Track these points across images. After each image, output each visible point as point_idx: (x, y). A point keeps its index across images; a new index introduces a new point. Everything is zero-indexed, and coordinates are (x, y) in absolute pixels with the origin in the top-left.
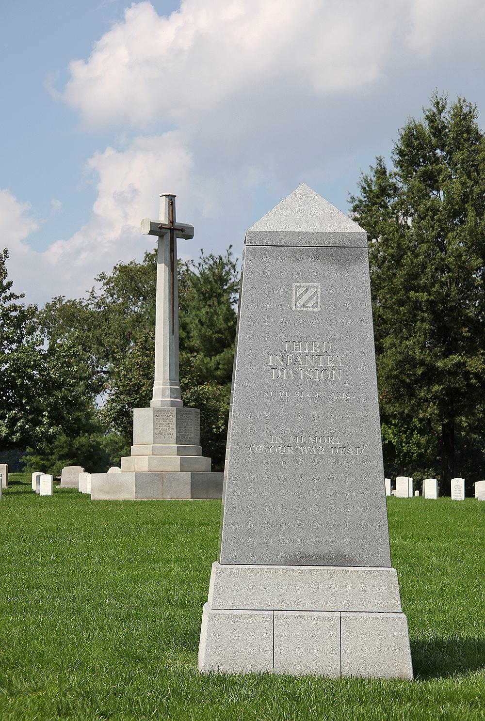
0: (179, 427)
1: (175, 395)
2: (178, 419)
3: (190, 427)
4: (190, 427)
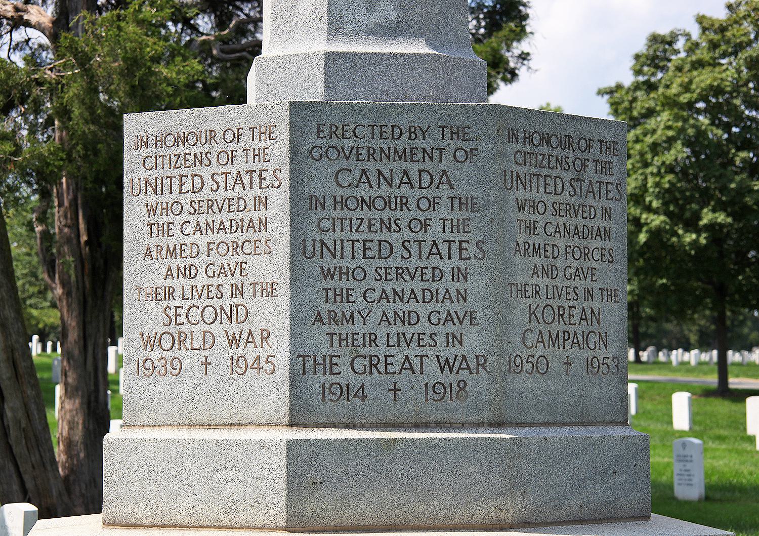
0: (328, 274)
1: (388, 12)
2: (318, 203)
3: (446, 266)
4: (446, 266)
